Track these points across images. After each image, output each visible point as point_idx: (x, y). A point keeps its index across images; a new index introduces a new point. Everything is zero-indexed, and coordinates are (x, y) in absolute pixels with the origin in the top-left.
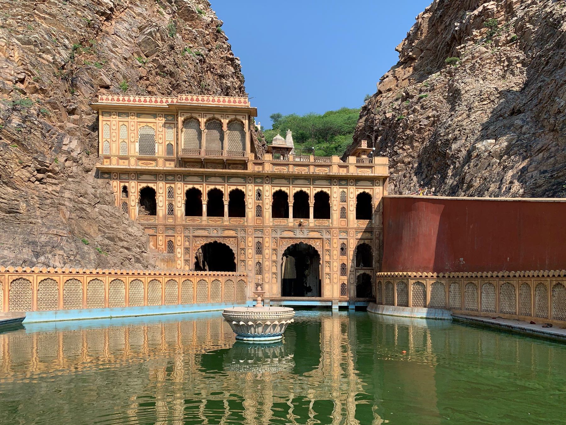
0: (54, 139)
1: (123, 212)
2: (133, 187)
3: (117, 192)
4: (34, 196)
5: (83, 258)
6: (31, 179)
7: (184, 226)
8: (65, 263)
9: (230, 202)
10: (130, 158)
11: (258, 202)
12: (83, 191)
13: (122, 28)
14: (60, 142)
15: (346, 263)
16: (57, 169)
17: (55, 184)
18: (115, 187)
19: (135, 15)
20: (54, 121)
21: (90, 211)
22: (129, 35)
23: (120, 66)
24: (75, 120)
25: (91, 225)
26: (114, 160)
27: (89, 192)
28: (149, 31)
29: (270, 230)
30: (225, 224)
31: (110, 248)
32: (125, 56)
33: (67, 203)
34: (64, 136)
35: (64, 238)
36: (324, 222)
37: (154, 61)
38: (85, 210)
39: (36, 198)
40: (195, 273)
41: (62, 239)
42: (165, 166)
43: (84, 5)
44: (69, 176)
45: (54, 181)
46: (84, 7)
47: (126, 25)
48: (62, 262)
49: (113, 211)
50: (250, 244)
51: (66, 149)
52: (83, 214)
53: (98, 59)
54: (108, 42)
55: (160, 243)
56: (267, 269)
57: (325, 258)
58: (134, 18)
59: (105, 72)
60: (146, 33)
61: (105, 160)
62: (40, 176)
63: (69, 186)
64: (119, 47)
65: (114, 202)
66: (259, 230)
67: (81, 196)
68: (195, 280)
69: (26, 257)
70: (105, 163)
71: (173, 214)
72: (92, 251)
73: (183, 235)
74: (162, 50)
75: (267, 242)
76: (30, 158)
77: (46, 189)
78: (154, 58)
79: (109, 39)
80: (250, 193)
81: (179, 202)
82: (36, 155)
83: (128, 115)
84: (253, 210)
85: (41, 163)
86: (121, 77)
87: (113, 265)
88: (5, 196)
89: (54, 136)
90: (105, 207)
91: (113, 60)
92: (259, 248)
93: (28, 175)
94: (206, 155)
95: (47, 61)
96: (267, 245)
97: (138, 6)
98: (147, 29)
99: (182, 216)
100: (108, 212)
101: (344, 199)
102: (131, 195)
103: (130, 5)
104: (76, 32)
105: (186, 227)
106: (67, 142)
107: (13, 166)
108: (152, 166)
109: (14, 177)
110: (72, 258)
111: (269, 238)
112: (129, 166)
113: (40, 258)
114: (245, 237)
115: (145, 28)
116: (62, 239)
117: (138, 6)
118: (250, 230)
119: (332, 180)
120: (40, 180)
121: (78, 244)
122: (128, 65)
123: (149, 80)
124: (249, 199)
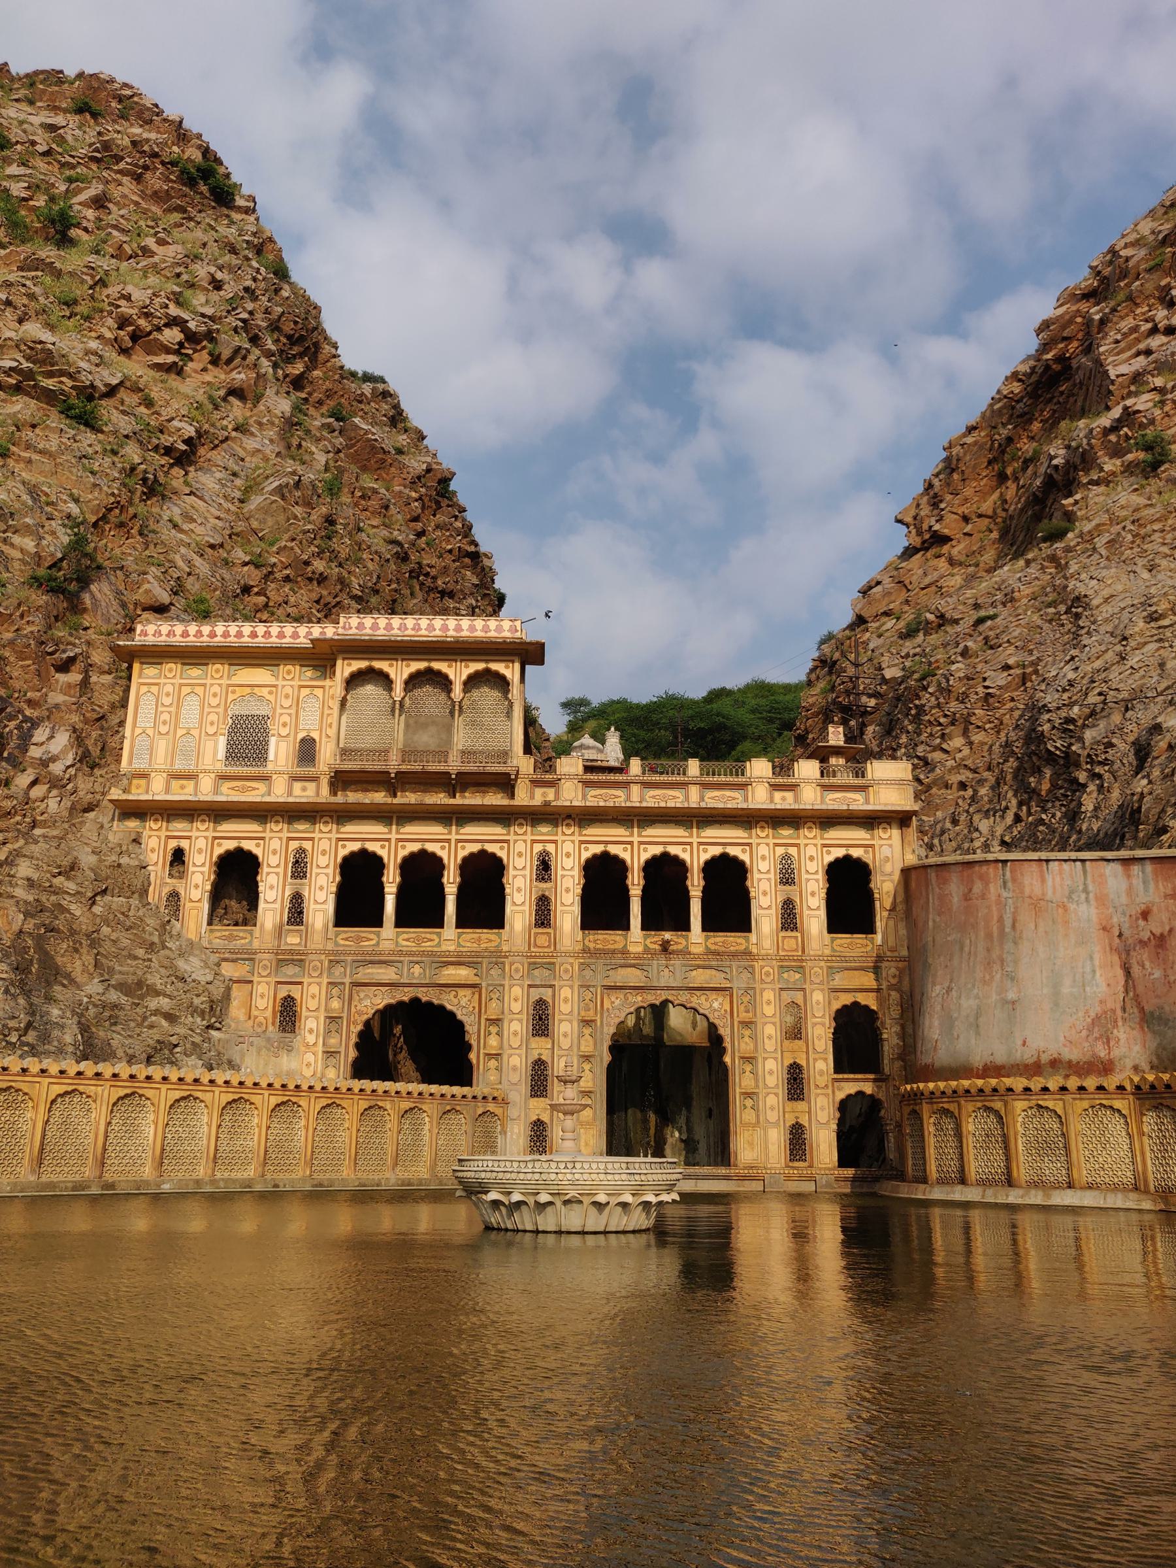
0: (11, 731)
1: (167, 918)
2: (200, 851)
5: (45, 1038)
10: (201, 776)
11: (543, 885)
12: (66, 863)
13: (209, 481)
14: (25, 740)
18: (153, 851)
19: (242, 454)
21: (78, 913)
23: (198, 561)
24: (69, 685)
25: (76, 950)
30: (444, 948)
32: (212, 541)
34: (35, 724)
36: (731, 941)
38: (68, 911)
40: (357, 1085)
42: (290, 793)
43: (125, 433)
44: (34, 824)
46: (127, 437)
51: (38, 755)
55: (261, 1003)
58: (243, 460)
61: (135, 782)
63: (33, 847)
65: (146, 891)
66: (542, 965)
67: (60, 874)
71: (301, 923)
72: (72, 1023)
73: (325, 980)
74: (304, 525)
75: (566, 1000)
78: (284, 543)
79: (175, 504)
81: (321, 888)
84: (527, 908)
91: (183, 550)
92: (540, 1019)
94: (403, 761)
95: (22, 550)
96: (565, 1008)
97: (252, 434)
102: (193, 873)
103: (234, 434)
104: (101, 489)
106: (43, 739)
108: (256, 794)
112: (196, 794)
114: (503, 985)
117: (252, 434)
118: (518, 966)
121: (35, 1000)
123: (265, 595)
124: (515, 877)
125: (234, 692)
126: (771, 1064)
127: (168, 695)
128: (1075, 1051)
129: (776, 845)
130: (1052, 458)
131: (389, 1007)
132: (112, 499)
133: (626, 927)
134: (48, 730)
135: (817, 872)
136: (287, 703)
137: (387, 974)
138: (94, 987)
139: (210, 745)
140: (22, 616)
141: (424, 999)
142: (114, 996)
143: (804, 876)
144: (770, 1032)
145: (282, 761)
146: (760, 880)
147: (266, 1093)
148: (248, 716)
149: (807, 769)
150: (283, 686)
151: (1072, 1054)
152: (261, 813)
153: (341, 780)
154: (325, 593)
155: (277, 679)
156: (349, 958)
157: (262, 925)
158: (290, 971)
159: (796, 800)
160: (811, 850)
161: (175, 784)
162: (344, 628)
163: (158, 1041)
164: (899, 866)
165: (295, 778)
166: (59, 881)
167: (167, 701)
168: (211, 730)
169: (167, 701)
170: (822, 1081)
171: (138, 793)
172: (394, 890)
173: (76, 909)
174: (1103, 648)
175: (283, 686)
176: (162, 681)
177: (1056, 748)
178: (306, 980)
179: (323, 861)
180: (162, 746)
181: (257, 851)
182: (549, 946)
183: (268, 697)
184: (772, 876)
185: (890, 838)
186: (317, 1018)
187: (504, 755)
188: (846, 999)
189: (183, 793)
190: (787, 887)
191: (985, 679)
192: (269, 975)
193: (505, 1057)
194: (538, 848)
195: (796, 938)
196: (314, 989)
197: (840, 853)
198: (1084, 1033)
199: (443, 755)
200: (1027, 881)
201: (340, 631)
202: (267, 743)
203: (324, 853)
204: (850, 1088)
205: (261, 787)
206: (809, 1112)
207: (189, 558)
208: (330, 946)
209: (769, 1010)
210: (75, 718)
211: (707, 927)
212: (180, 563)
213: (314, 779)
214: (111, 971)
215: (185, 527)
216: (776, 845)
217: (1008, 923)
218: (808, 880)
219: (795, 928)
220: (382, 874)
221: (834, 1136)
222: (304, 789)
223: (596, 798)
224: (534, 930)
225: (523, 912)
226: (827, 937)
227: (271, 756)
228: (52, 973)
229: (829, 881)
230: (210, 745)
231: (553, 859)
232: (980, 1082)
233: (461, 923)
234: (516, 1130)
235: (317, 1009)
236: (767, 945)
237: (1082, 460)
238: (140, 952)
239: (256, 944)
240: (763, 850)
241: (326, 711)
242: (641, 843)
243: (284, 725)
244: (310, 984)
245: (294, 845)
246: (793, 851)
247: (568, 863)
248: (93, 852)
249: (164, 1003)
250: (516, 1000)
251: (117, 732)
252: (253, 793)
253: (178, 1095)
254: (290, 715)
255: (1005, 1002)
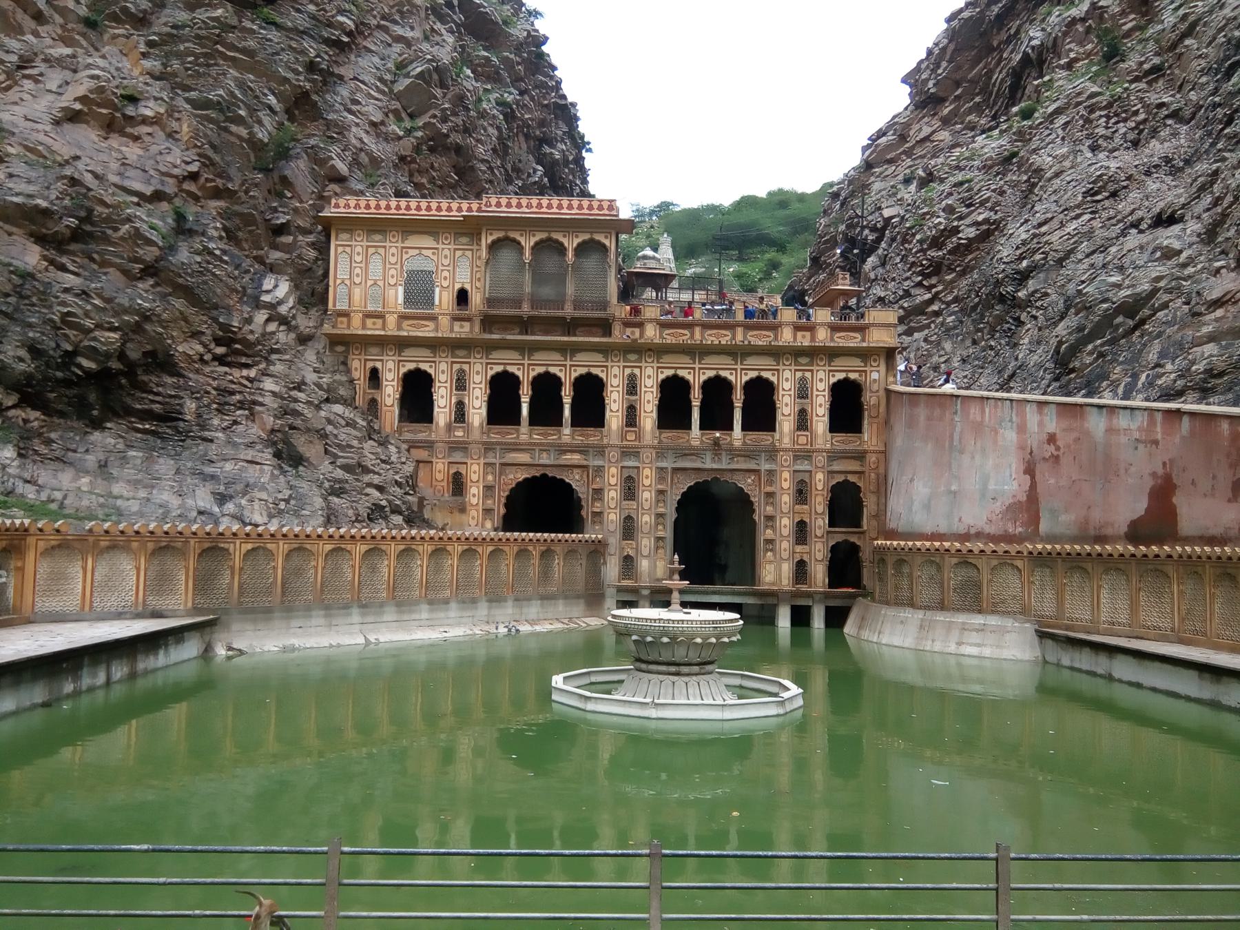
3: (359, 379)
4: (209, 389)
6: (205, 358)
7: (484, 443)
8: (271, 516)
9: (574, 399)
12: (298, 379)
15: (808, 520)
16: (250, 337)
17: (247, 366)
20: (247, 248)
22: (381, 80)
25: (311, 442)
26: (356, 320)
27: (308, 380)
28: (419, 69)
29: (654, 455)
31: (347, 486)
33: (268, 400)
34: (263, 276)
35: (266, 467)
36: (763, 438)
37: (426, 126)
38: (302, 415)
39: (214, 392)
41: (262, 471)
42: (452, 331)
44: (273, 351)
45: (244, 360)
47: (376, 60)
48: (265, 513)
49: (352, 415)
50: (613, 481)
52: (298, 422)
53: (325, 128)
54: (344, 92)
56: (646, 529)
57: (761, 510)
59: (340, 151)
60: (412, 73)
61: (340, 319)
62: (220, 350)
63: (271, 368)
64: (364, 103)
65: (354, 399)
68: (511, 550)
69: (201, 504)
70: (339, 326)
71: (464, 422)
75: (647, 477)
76: (205, 318)
77: (231, 375)
80: (615, 382)
82: (215, 313)
83: (383, 232)
84: (620, 414)
85: (225, 327)
86: (367, 160)
87: (354, 518)
88: (160, 389)
89: (247, 278)
90: (338, 408)
91: (354, 129)
93: (200, 349)
96: (647, 482)
98: (414, 65)
99: (481, 424)
100: (343, 418)
101: (803, 392)
105: (488, 447)
106: (270, 287)
107: (175, 334)
108: (427, 331)
109: (177, 354)
110: (282, 505)
111: (651, 468)
113: (226, 507)
115: (412, 62)
116: (262, 471)
118: (614, 454)
119: (776, 353)
120: (221, 360)
122: (378, 136)
124: (612, 392)
125: (407, 253)
126: (785, 521)
127: (358, 254)
128: (993, 528)
129: (796, 370)
130: (1031, 39)
131: (526, 480)
132: (299, 91)
133: (689, 427)
134: (273, 280)
135: (824, 390)
136: (446, 262)
137: (523, 458)
138: (325, 466)
139: (392, 292)
140: (246, 192)
141: (550, 475)
142: (339, 474)
143: (815, 393)
144: (786, 499)
145: (445, 306)
146: (783, 395)
147: (456, 544)
148: (418, 271)
149: (822, 315)
150: (443, 249)
151: (989, 529)
152: (434, 345)
153: (488, 322)
154: (460, 160)
155: (438, 243)
156: (498, 447)
157: (437, 423)
158: (458, 457)
159: (813, 339)
160: (821, 375)
161: (369, 322)
162: (486, 205)
163: (373, 504)
164: (883, 385)
165: (456, 319)
166: (295, 393)
167: (358, 259)
168: (392, 281)
169: (358, 259)
170: (819, 533)
171: (342, 328)
172: (528, 400)
173: (308, 412)
174: (1049, 215)
175: (443, 249)
176: (354, 243)
177: (1008, 292)
178: (469, 462)
179: (477, 378)
180: (357, 292)
181: (431, 371)
182: (635, 440)
183: (432, 257)
184: (792, 393)
185: (878, 366)
186: (478, 487)
187: (604, 305)
188: (841, 478)
189: (374, 329)
190: (803, 401)
191: (959, 232)
192: (444, 458)
193: (606, 515)
194: (628, 371)
195: (807, 436)
196: (475, 467)
197: (841, 376)
198: (1000, 516)
199: (560, 304)
200: (972, 411)
201: (484, 208)
202: (433, 292)
203: (478, 373)
204: (839, 538)
205: (431, 325)
206: (809, 553)
207: (359, 136)
208: (485, 438)
209: (786, 485)
210: (290, 271)
211: (745, 428)
212: (354, 141)
213: (469, 319)
214: (336, 456)
215: (354, 108)
216: (796, 370)
217: (956, 437)
218: (817, 396)
219: (806, 429)
220: (519, 389)
221: (826, 569)
222: (462, 327)
223: (670, 337)
224: (626, 429)
225: (618, 416)
226: (829, 435)
227: (437, 302)
228: (297, 460)
229: (833, 396)
230: (392, 292)
231: (638, 379)
232: (928, 544)
233: (575, 423)
234: (613, 561)
235: (478, 481)
236: (786, 442)
237: (1052, 48)
238: (355, 443)
239: (433, 437)
240: (787, 374)
241: (475, 269)
242: (700, 369)
243: (445, 278)
244: (472, 464)
245: (456, 367)
246: (808, 375)
247: (649, 382)
248: (315, 371)
249: (376, 480)
250: (613, 476)
251: (322, 281)
252: (427, 329)
253: (402, 547)
254: (449, 271)
255: (950, 492)
